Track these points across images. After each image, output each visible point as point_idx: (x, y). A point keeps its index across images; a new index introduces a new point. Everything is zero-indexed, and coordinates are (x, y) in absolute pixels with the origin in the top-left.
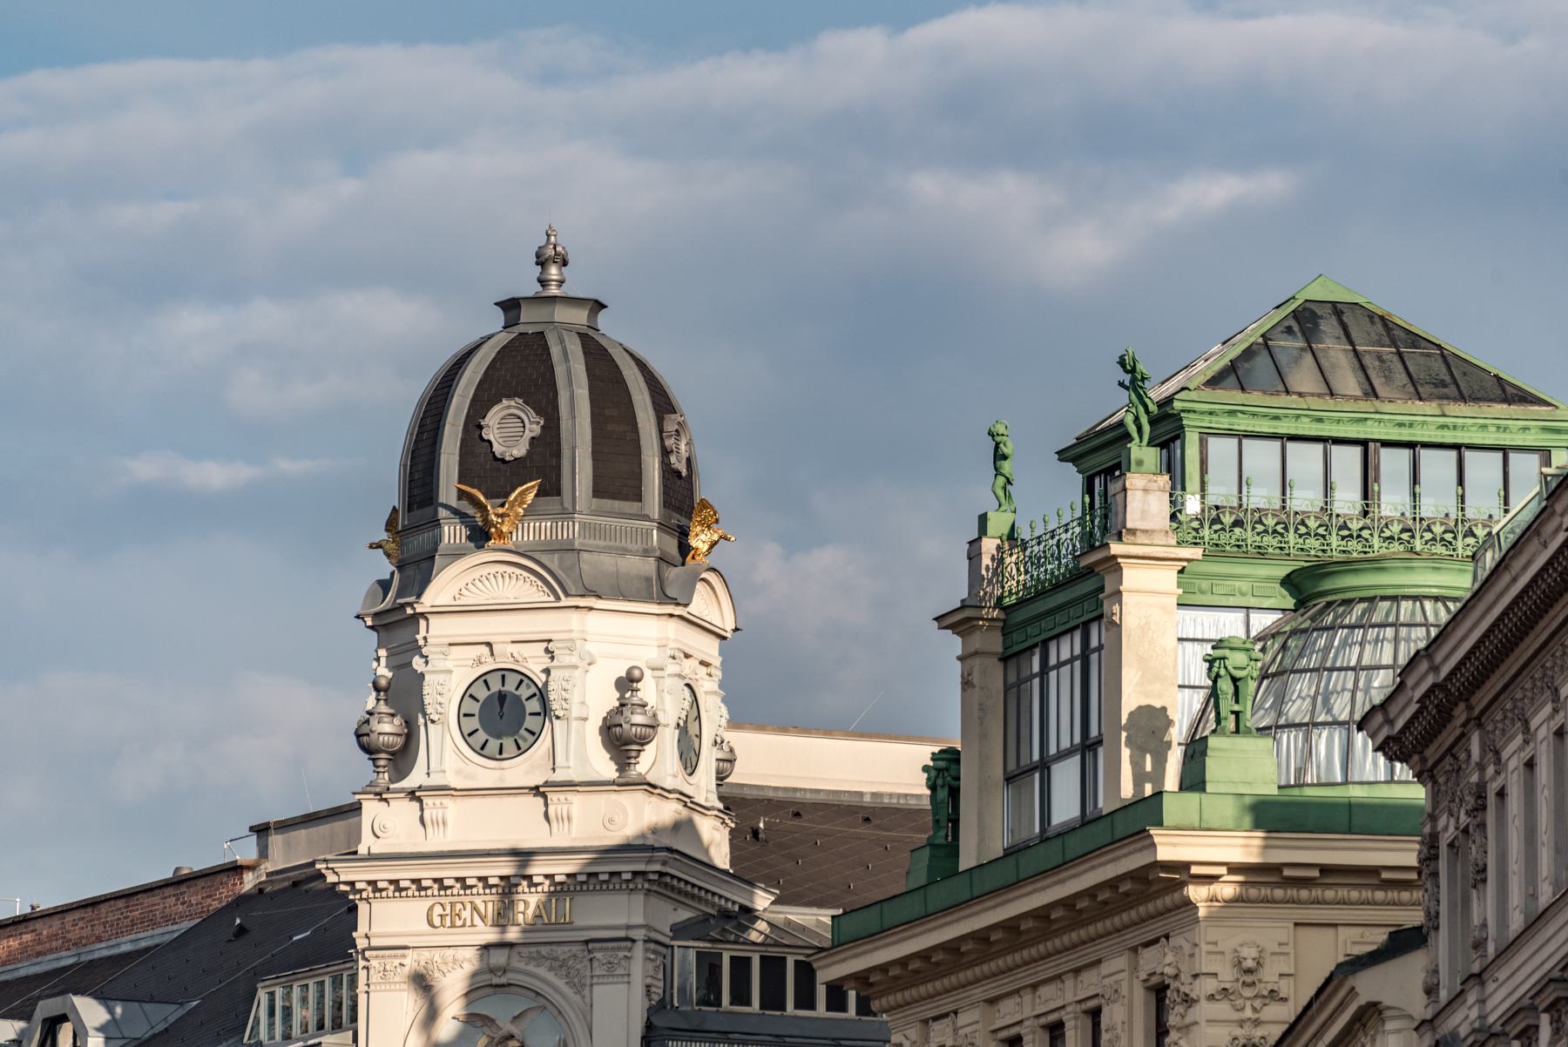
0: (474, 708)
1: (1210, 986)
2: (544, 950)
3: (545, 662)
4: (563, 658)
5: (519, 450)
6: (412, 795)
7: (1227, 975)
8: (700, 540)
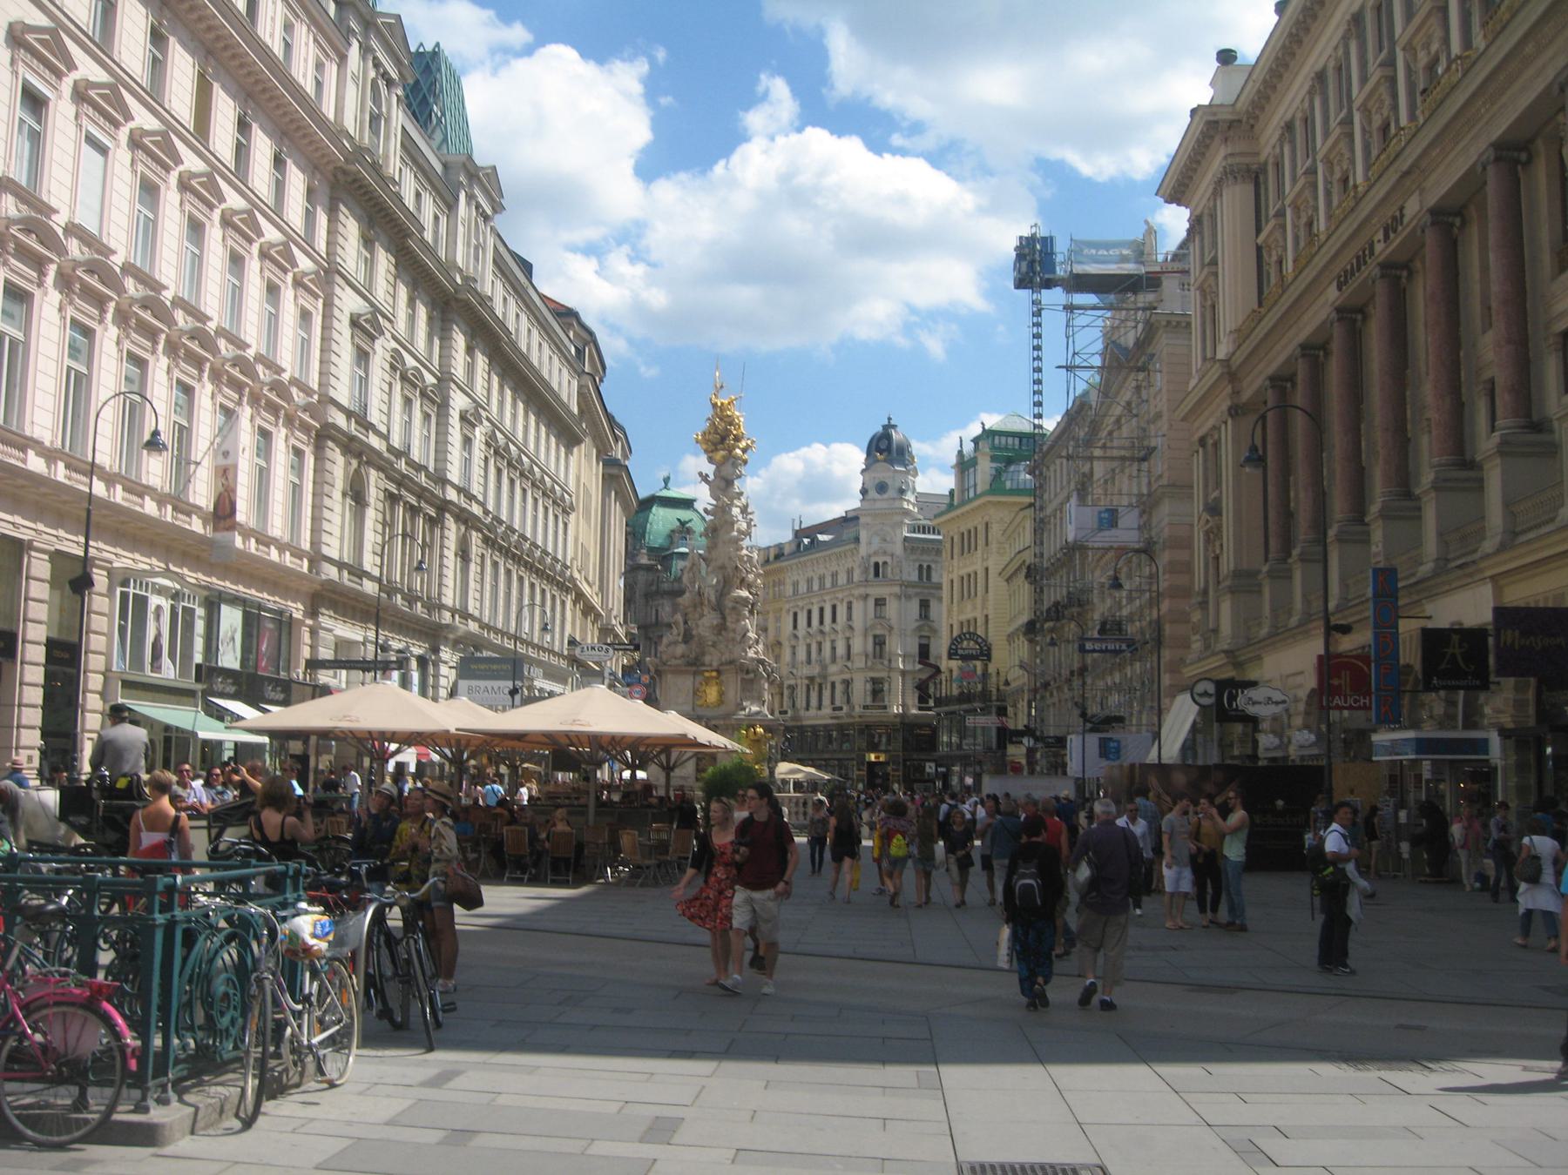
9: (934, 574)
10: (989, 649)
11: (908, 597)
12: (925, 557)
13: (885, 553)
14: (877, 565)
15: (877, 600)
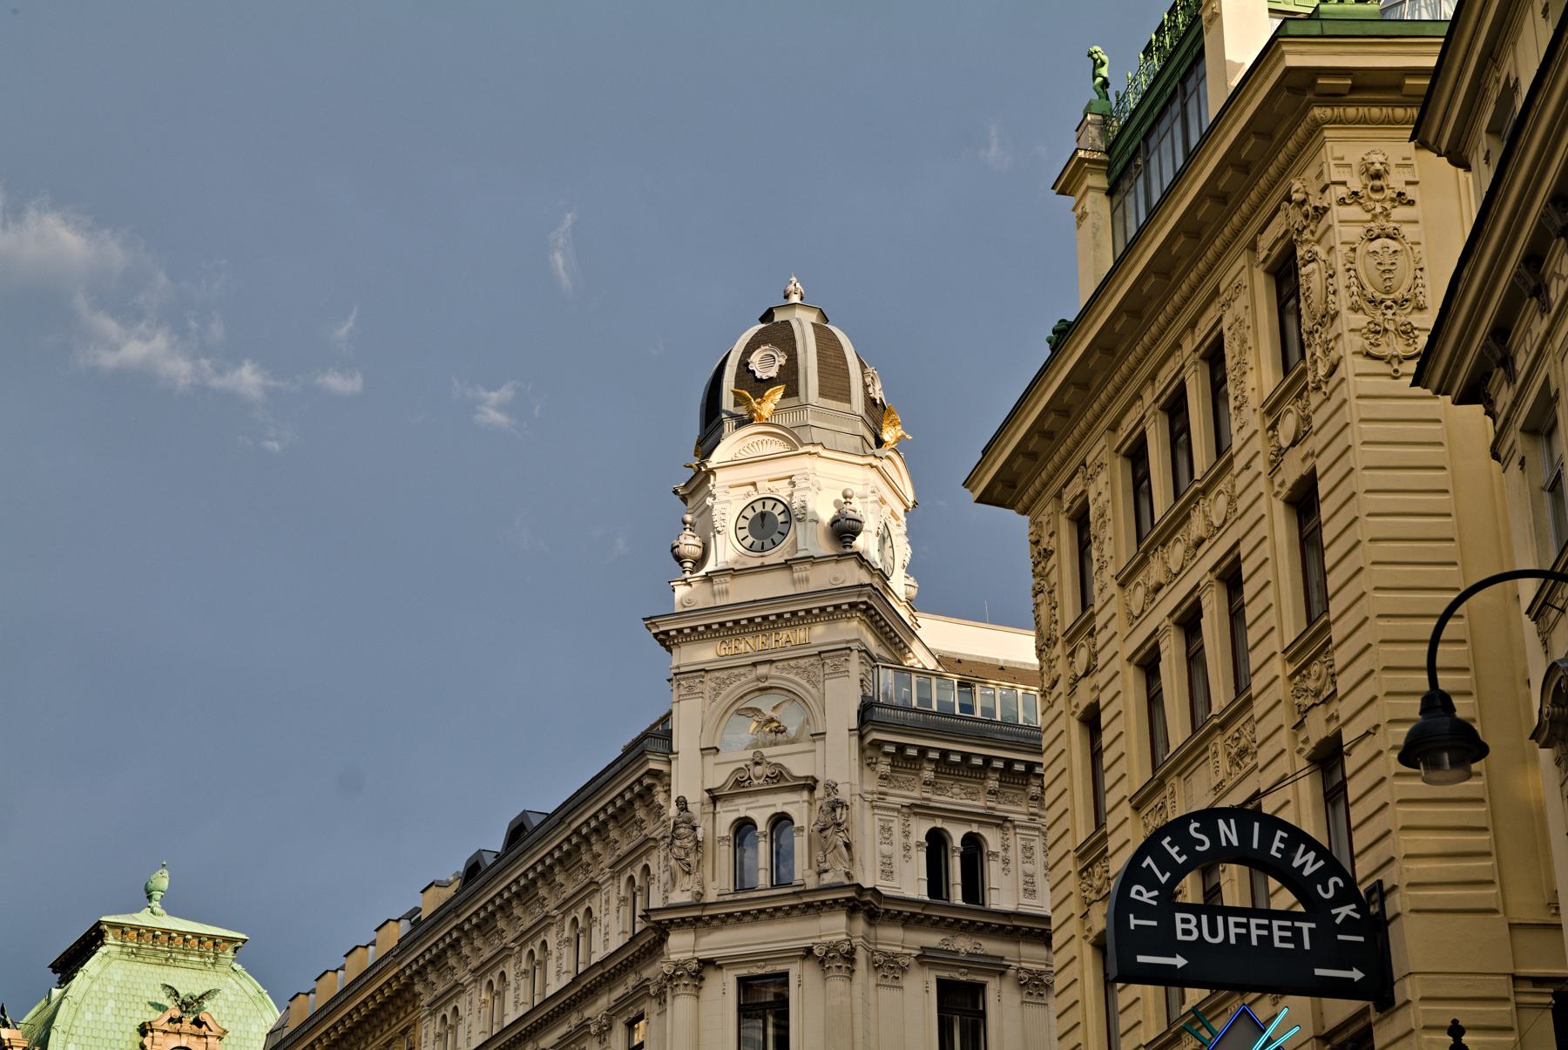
0: (745, 523)
1: (1341, 191)
2: (792, 663)
3: (789, 489)
4: (800, 484)
5: (773, 373)
6: (708, 578)
7: (1356, 184)
8: (889, 435)
9: (993, 873)
10: (1376, 926)
11: (889, 967)
12: (954, 797)
13: (779, 780)
14: (743, 827)
15: (743, 983)
